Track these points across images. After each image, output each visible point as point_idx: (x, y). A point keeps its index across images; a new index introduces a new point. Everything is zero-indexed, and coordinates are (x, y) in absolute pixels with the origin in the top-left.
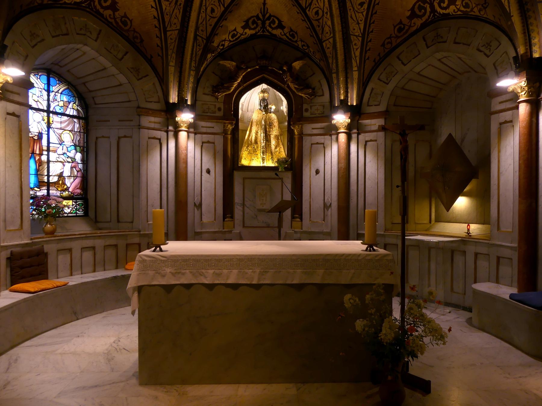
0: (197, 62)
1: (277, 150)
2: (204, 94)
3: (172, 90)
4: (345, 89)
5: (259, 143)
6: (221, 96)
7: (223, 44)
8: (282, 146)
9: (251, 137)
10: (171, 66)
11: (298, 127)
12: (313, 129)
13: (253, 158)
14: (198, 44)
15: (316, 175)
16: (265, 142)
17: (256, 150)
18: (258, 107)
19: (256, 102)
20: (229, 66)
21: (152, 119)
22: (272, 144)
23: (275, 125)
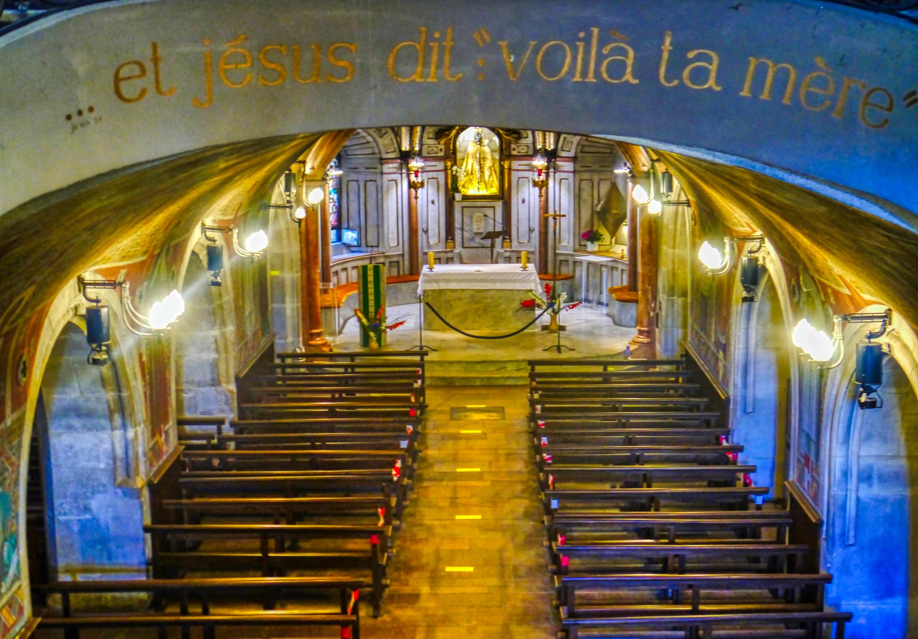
2: (429, 138)
6: (442, 142)
21: (391, 165)
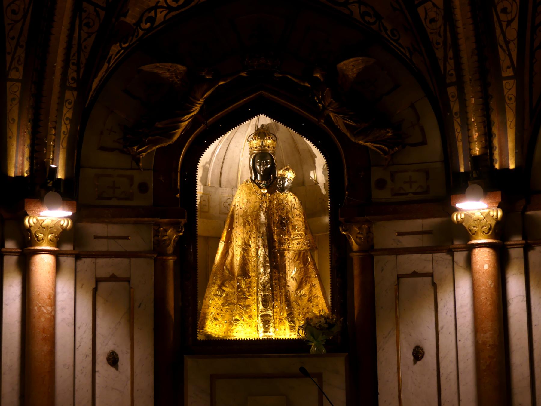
0: (82, 66)
1: (303, 292)
2: (103, 149)
3: (15, 143)
4: (485, 127)
5: (252, 274)
7: (151, 17)
8: (316, 282)
9: (229, 258)
10: (12, 80)
11: (359, 228)
12: (400, 234)
13: (237, 317)
14: (83, 23)
15: (415, 363)
16: (269, 270)
17: (244, 294)
18: (247, 174)
19: (241, 159)
20: (168, 74)
22: (287, 276)
23: (295, 223)
